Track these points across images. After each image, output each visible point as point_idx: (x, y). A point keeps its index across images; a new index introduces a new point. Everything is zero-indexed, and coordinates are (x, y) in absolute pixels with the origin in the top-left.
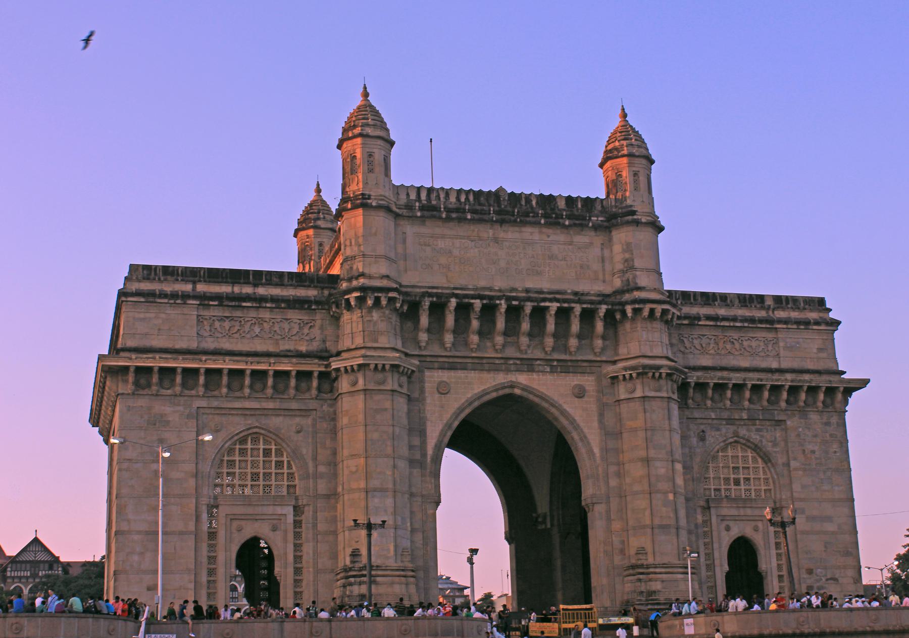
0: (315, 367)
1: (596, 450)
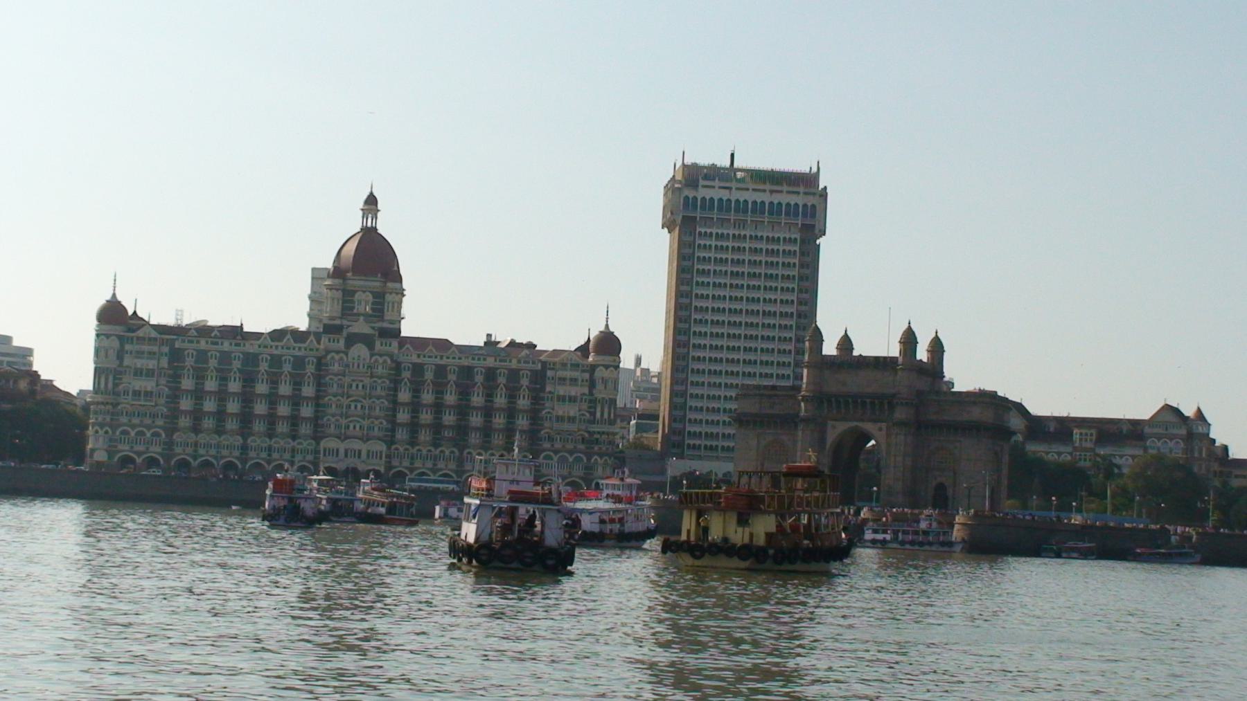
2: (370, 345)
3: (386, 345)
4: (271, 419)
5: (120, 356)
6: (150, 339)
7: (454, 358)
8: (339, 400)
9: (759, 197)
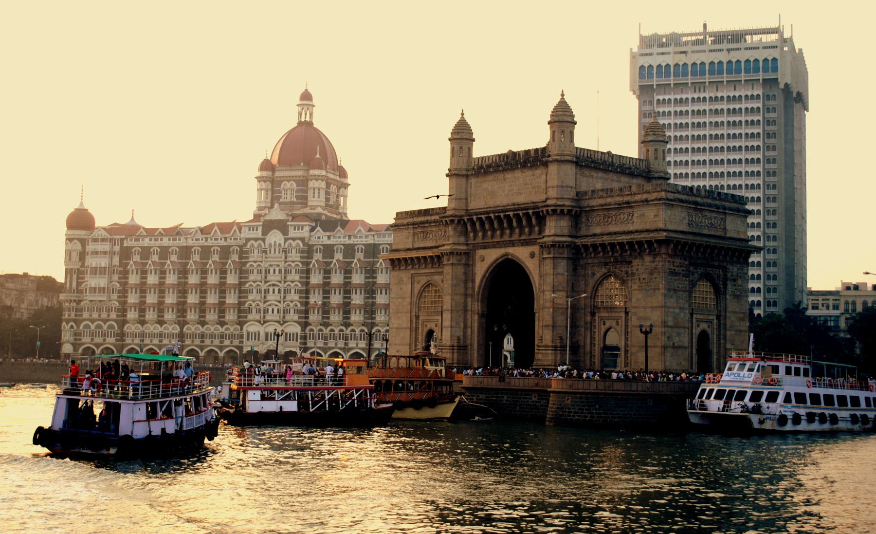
1: (537, 285)
2: (285, 232)
3: (298, 230)
4: (202, 308)
5: (82, 256)
6: (103, 240)
7: (361, 237)
8: (258, 285)
9: (716, 57)
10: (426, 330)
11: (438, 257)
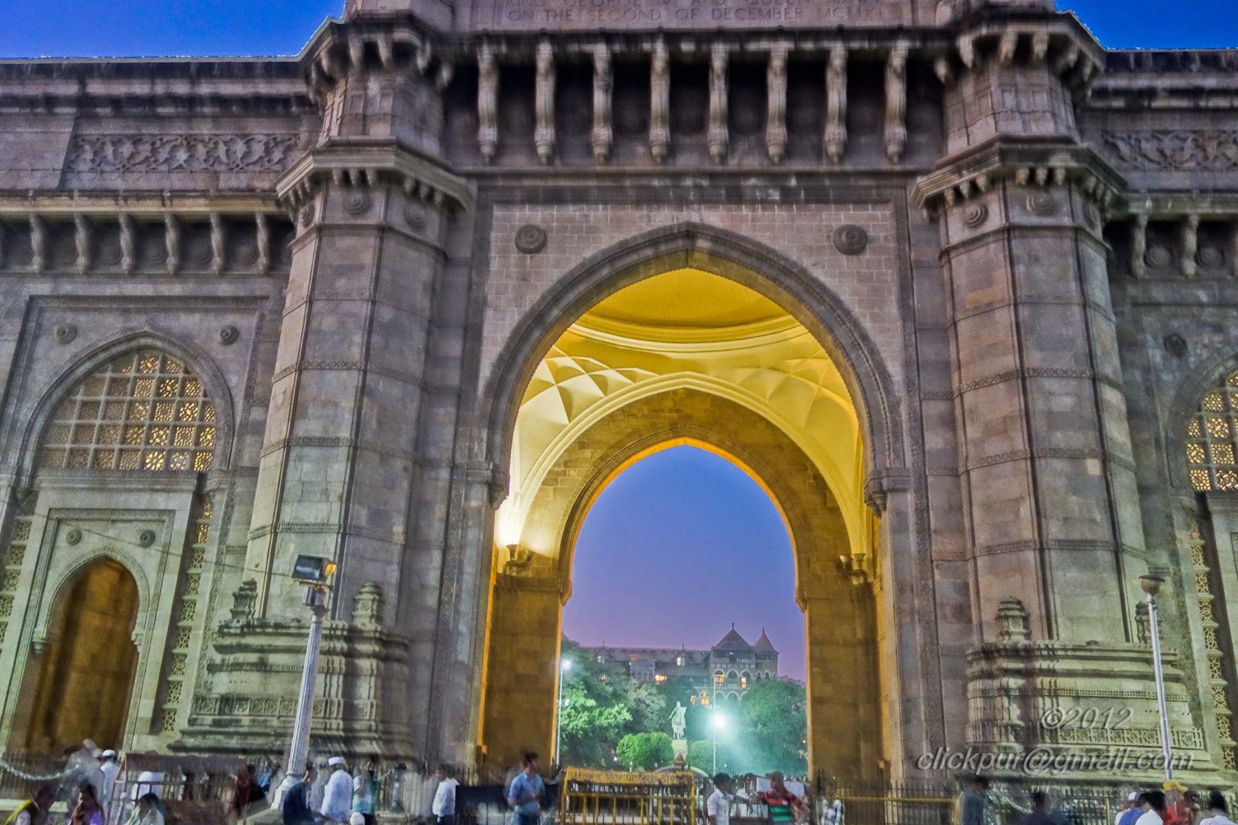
0: (259, 209)
10: (66, 559)
11: (237, 227)
